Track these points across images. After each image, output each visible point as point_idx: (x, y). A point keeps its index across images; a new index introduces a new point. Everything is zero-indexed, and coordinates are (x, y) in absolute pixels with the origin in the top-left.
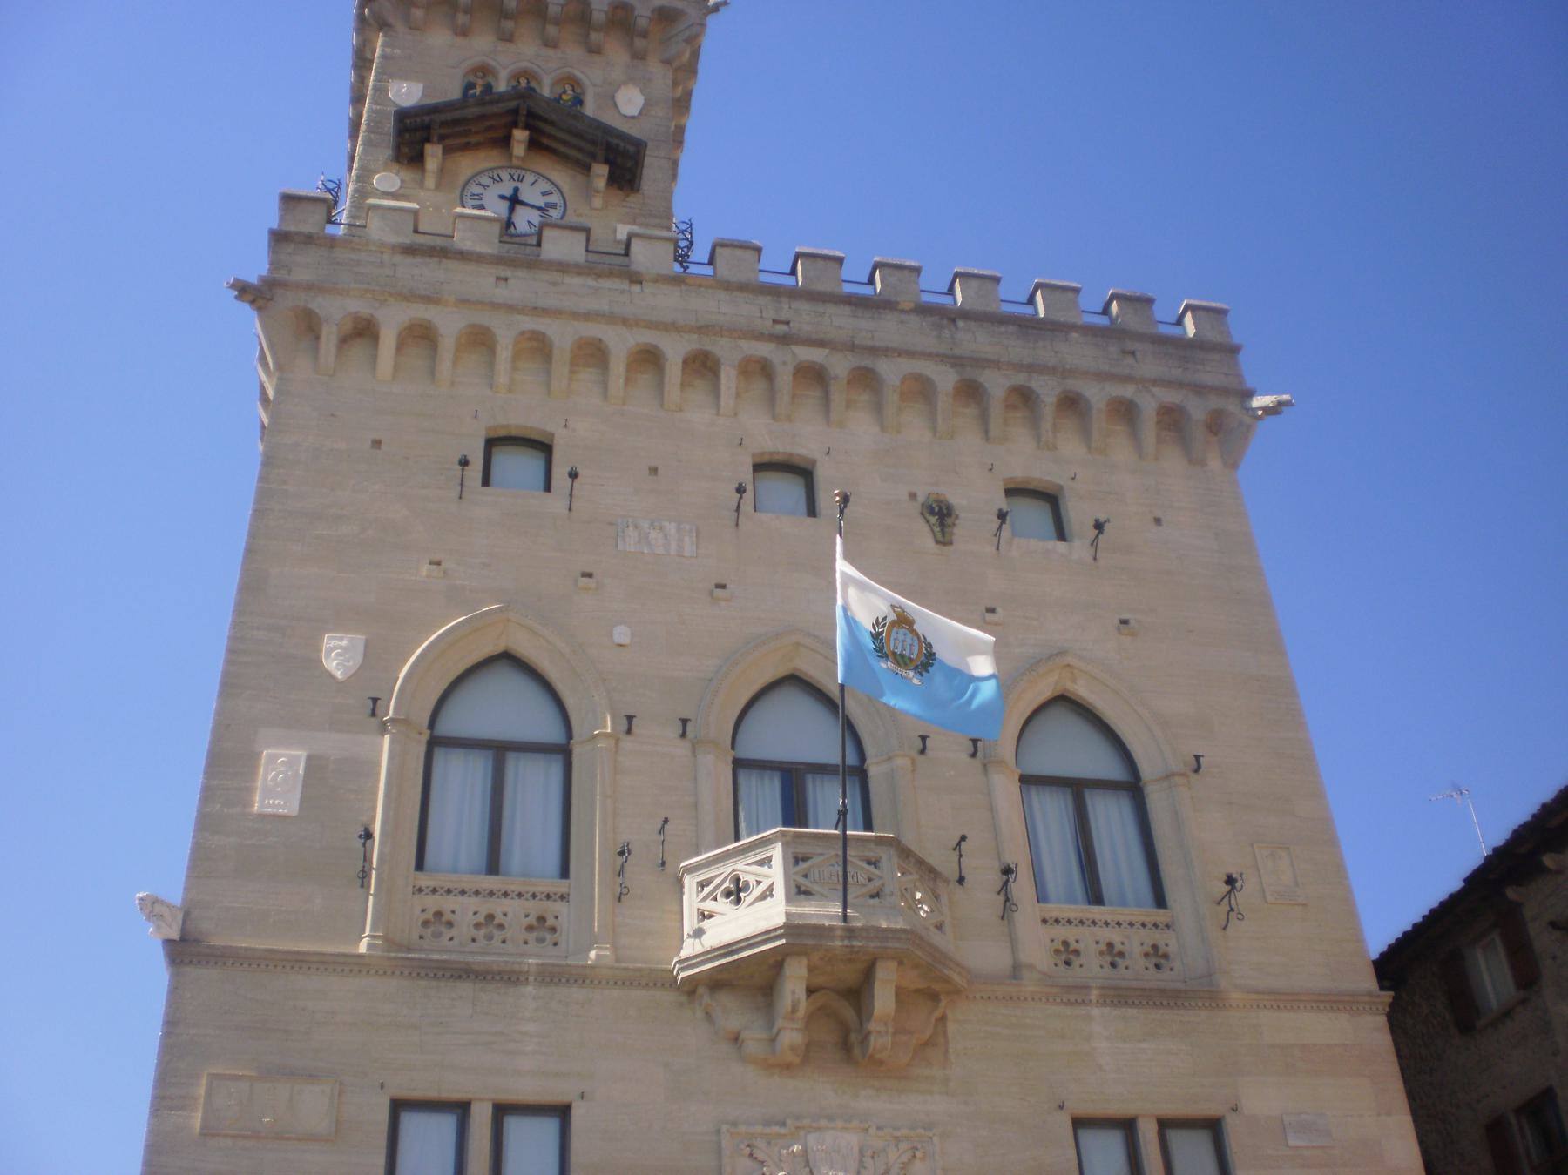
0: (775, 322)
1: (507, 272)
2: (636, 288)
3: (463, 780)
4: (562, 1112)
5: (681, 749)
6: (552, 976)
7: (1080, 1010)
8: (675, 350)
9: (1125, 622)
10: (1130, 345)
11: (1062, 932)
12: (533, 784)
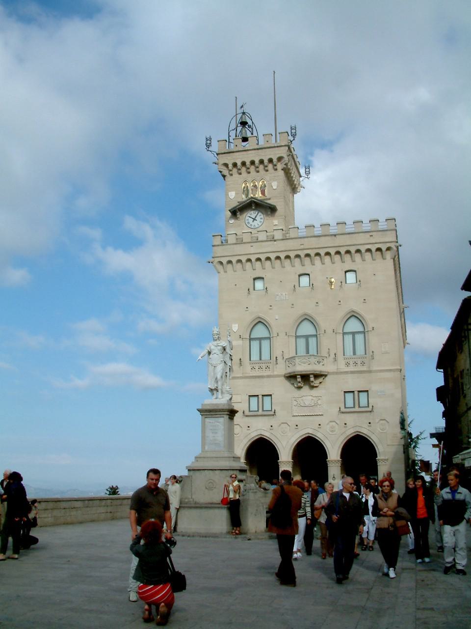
0: (301, 245)
1: (252, 244)
2: (275, 243)
3: (255, 345)
4: (271, 395)
5: (286, 337)
6: (268, 376)
7: (347, 375)
8: (282, 256)
9: (365, 300)
10: (371, 234)
11: (348, 360)
12: (265, 344)
